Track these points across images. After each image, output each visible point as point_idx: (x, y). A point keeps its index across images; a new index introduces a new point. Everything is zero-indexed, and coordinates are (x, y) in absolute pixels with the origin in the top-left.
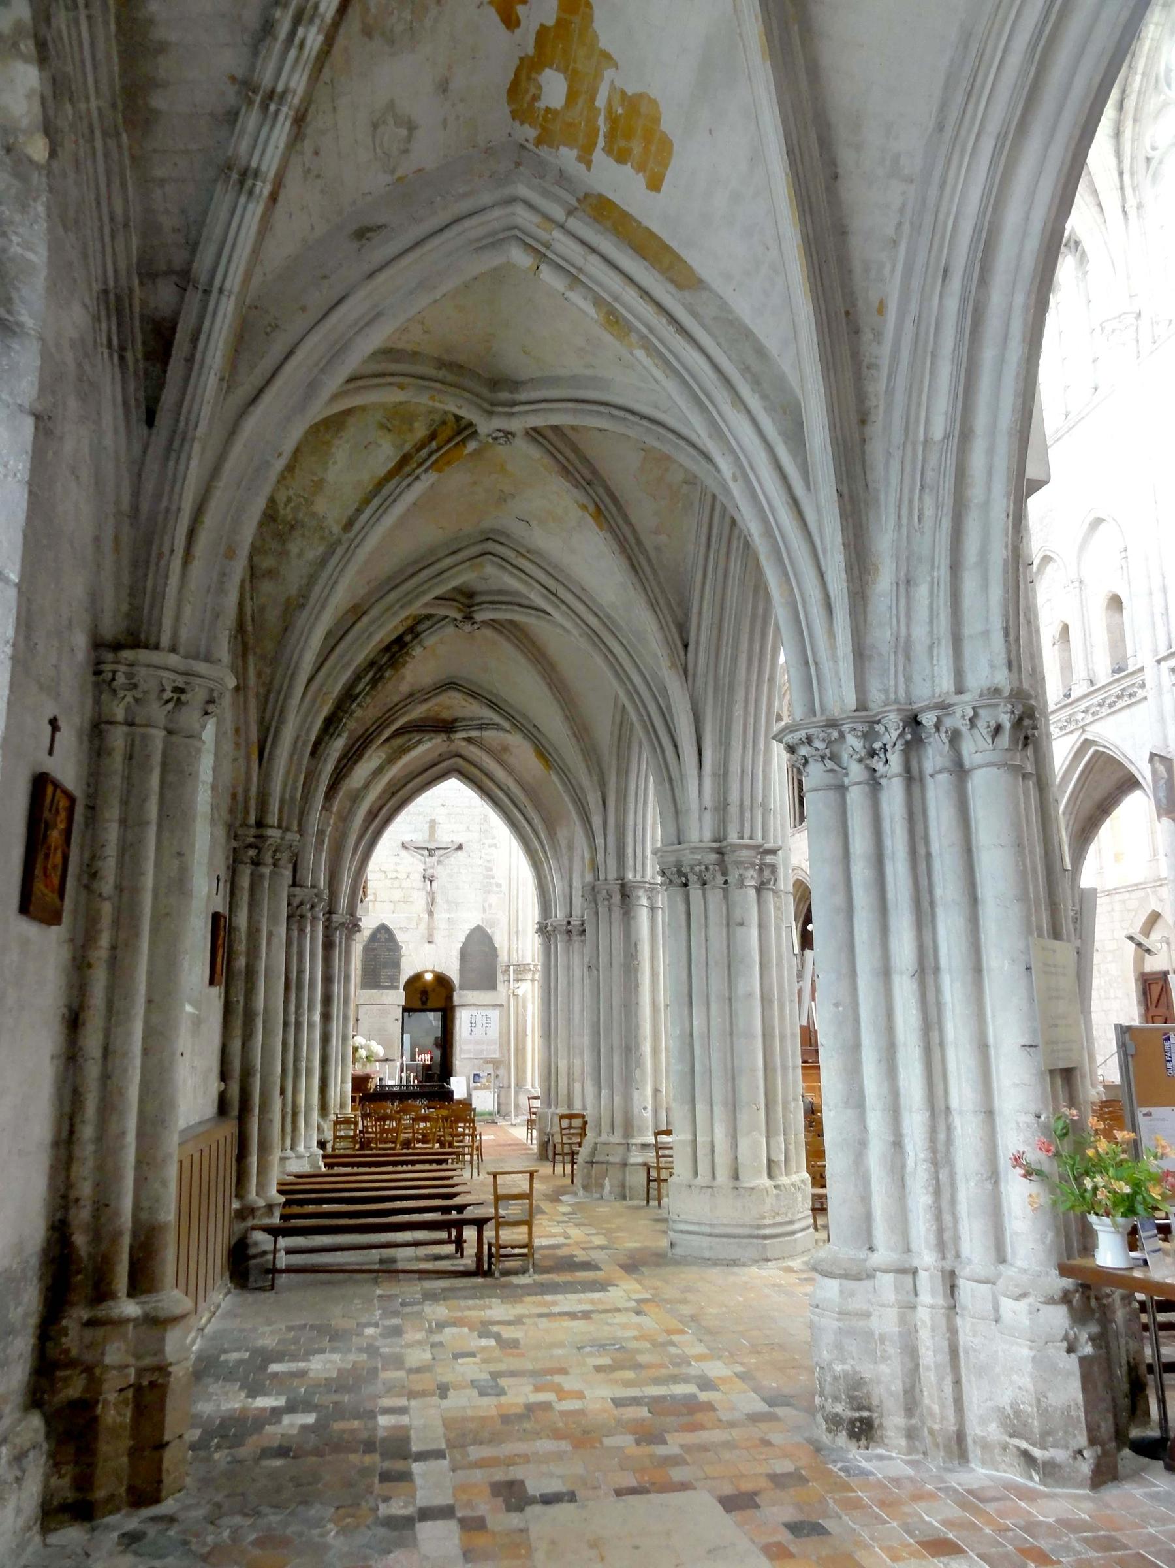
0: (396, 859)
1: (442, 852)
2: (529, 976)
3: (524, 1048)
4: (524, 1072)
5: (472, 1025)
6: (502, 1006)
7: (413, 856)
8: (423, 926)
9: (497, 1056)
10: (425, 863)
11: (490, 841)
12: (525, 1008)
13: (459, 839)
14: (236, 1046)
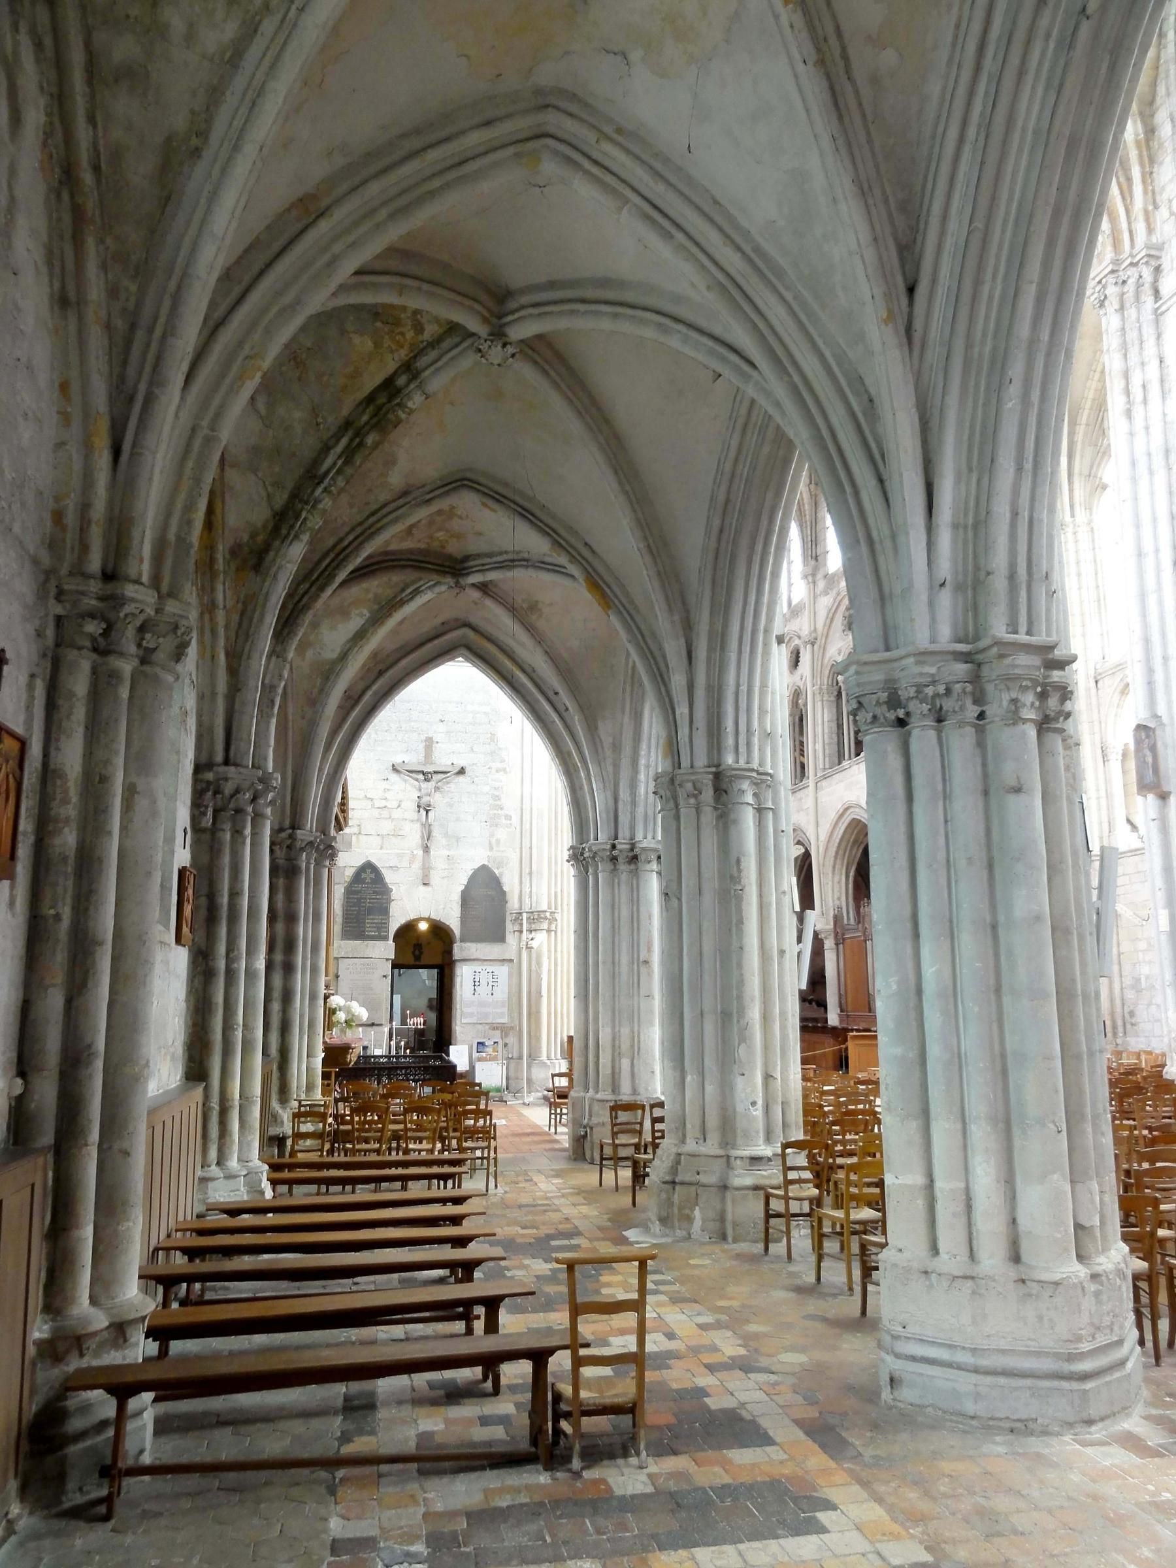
0: (385, 785)
1: (443, 776)
2: (545, 926)
3: (538, 1012)
4: (538, 1039)
5: (476, 984)
6: (511, 961)
7: (405, 781)
8: (417, 865)
9: (505, 1020)
10: (420, 790)
11: (499, 765)
12: (539, 964)
13: (460, 762)
14: (53, 1002)
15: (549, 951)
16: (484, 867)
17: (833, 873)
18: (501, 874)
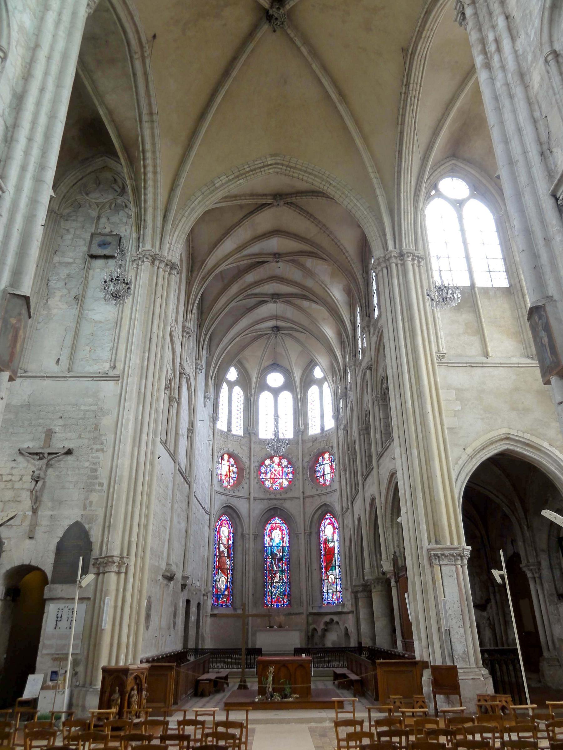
0: (13, 464)
2: (114, 568)
5: (58, 619)
6: (89, 599)
7: (28, 461)
8: (27, 523)
11: (98, 446)
13: (69, 445)
15: (117, 590)
16: (77, 524)
17: (392, 528)
18: (90, 528)
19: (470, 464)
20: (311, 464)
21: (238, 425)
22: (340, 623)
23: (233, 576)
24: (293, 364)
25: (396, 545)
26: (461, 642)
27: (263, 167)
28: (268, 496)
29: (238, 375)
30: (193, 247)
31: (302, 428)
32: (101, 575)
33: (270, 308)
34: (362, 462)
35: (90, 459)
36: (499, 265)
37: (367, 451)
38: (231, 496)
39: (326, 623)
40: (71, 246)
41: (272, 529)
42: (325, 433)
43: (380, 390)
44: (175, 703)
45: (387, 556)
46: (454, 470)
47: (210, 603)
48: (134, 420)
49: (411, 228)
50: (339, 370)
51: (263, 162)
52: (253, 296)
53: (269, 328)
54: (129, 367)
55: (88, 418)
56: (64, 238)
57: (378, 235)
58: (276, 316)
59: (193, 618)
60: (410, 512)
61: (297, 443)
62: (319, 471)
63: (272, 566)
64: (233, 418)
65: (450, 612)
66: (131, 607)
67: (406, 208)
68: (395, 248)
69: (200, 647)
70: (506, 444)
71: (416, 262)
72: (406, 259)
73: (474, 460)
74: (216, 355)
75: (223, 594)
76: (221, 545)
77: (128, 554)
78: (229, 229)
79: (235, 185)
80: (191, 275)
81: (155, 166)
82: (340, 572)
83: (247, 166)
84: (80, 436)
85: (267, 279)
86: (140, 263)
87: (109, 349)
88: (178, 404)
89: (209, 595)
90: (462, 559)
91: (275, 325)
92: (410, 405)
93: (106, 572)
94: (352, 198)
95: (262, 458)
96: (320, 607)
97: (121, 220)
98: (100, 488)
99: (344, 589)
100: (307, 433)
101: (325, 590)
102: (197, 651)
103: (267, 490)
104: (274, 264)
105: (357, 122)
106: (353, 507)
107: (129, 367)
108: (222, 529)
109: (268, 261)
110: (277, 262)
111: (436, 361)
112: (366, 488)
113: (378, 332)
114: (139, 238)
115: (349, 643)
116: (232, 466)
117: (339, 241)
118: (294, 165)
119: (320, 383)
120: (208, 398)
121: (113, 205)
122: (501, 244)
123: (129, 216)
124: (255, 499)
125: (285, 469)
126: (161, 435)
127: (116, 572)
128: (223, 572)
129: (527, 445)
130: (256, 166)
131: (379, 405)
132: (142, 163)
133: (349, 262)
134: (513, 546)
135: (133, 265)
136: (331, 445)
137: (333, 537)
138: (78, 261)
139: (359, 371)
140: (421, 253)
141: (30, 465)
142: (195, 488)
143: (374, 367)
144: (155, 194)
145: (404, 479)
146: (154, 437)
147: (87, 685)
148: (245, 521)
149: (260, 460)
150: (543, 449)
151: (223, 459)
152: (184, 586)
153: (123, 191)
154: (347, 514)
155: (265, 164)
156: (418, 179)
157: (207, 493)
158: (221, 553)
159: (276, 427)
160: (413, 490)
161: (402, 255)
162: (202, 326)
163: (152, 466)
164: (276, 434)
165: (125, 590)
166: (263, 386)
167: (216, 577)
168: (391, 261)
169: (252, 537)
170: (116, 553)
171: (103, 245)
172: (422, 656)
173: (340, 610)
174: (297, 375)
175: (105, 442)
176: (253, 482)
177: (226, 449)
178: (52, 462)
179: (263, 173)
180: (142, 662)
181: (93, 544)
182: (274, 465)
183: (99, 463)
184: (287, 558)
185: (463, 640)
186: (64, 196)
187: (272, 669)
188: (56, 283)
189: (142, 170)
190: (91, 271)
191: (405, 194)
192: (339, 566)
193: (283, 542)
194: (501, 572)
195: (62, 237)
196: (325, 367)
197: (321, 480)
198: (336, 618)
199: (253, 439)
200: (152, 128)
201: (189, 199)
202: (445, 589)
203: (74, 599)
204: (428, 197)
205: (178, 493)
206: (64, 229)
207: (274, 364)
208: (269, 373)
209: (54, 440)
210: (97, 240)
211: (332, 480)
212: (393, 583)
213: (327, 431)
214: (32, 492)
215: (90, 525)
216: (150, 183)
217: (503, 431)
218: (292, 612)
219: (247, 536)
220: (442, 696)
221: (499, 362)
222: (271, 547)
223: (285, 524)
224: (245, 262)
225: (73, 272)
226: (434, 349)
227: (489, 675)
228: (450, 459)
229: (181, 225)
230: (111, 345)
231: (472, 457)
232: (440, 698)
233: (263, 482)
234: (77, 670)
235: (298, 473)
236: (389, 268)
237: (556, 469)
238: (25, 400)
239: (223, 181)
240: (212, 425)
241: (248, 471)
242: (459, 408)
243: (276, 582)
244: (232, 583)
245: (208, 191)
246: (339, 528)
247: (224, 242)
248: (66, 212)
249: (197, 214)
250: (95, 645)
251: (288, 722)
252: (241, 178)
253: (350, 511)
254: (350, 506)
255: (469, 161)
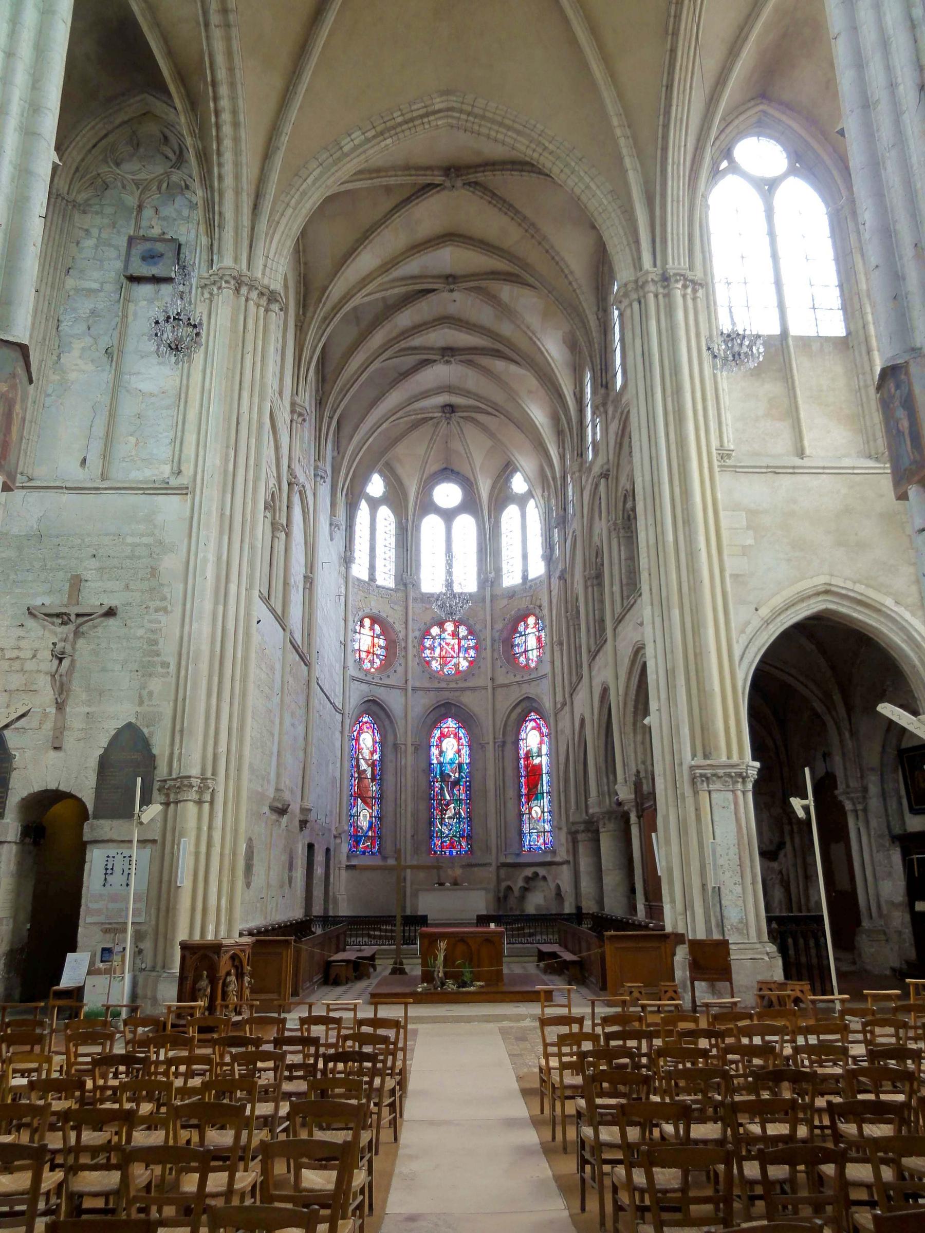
0: (20, 632)
2: (193, 795)
5: (108, 871)
6: (154, 841)
7: (44, 627)
8: (49, 725)
11: (158, 603)
15: (199, 829)
16: (129, 725)
18: (151, 733)
19: (765, 633)
20: (505, 634)
21: (386, 570)
22: (549, 878)
23: (380, 808)
24: (478, 469)
25: (640, 761)
26: (736, 905)
27: (427, 115)
28: (437, 685)
29: (385, 487)
30: (305, 264)
31: (492, 575)
32: (172, 805)
33: (438, 373)
34: (588, 630)
35: (147, 625)
36: (832, 297)
37: (596, 612)
38: (377, 685)
39: (528, 879)
40: (94, 259)
41: (443, 736)
42: (529, 584)
43: (621, 513)
44: (295, 993)
45: (625, 778)
46: (738, 642)
47: (345, 848)
48: (215, 559)
49: (684, 230)
50: (554, 478)
51: (426, 107)
52: (410, 352)
53: (436, 407)
54: (203, 471)
55: (139, 558)
56: (81, 245)
57: (625, 243)
58: (449, 387)
59: (319, 871)
60: (664, 710)
61: (484, 599)
62: (518, 645)
63: (442, 794)
64: (377, 559)
65: (721, 861)
66: (222, 855)
67: (675, 192)
68: (655, 265)
69: (331, 914)
70: (825, 601)
71: (689, 291)
72: (673, 285)
73: (771, 626)
74: (349, 452)
75: (366, 836)
76: (362, 761)
77: (214, 773)
78: (367, 231)
79: (376, 148)
80: (304, 314)
81: (234, 112)
82: (550, 802)
83: (399, 113)
84: (127, 586)
85: (434, 320)
86: (215, 291)
87: (168, 441)
88: (287, 534)
89: (343, 836)
90: (744, 782)
91: (448, 402)
92: (670, 537)
93: (180, 801)
94: (582, 173)
95: (425, 624)
96: (518, 855)
97: (179, 212)
98: (164, 670)
99: (556, 828)
100: (500, 584)
101: (526, 829)
102: (325, 920)
103: (433, 676)
104: (446, 295)
105: (594, 31)
106: (572, 703)
107: (203, 471)
108: (362, 737)
109: (434, 290)
110: (452, 291)
111: (716, 463)
112: (593, 673)
113: (622, 413)
114: (212, 245)
115: (563, 909)
116: (378, 637)
117: (558, 253)
118: (481, 112)
119: (522, 501)
120: (337, 525)
121: (165, 185)
122: (837, 259)
123: (193, 206)
124: (414, 689)
125: (463, 642)
126: (260, 585)
127: (195, 802)
128: (364, 802)
129: (860, 602)
130: (415, 114)
131: (619, 538)
132: (212, 105)
133: (574, 290)
134: (825, 761)
135: (203, 294)
136: (538, 603)
137: (540, 749)
138: (108, 287)
139: (587, 480)
140: (698, 275)
141: (47, 634)
142: (317, 671)
143: (613, 473)
144: (237, 164)
145: (656, 657)
146: (249, 589)
147: (158, 968)
148: (400, 723)
149: (423, 627)
150: (884, 609)
151: (362, 626)
152: (303, 824)
153: (180, 160)
154: (563, 713)
155: (430, 109)
156: (698, 140)
157: (337, 680)
158: (361, 773)
159: (449, 573)
160: (670, 674)
161: (665, 279)
162: (323, 402)
163: (247, 634)
164: (449, 584)
165: (210, 828)
166: (427, 506)
167: (355, 809)
168: (646, 289)
169: (410, 749)
170: (195, 771)
171: (150, 257)
172: (675, 925)
173: (548, 858)
174: (484, 487)
175: (169, 596)
176: (412, 662)
177: (367, 610)
178: (84, 628)
179: (427, 126)
180: (241, 935)
181: (157, 758)
182: (444, 635)
183: (161, 630)
184: (466, 782)
185: (740, 903)
186: (77, 169)
187: (443, 945)
188: (71, 326)
189: (213, 119)
190: (131, 307)
191: (675, 166)
192: (548, 793)
193: (460, 756)
194: (805, 802)
195: (78, 243)
196: (530, 475)
197: (522, 659)
198: (542, 871)
199: (412, 594)
200: (228, 39)
201: (297, 175)
202: (716, 827)
203: (131, 842)
204: (716, 173)
205: (291, 680)
206: (80, 228)
207: (446, 469)
208: (437, 483)
209: (84, 593)
210: (140, 249)
211: (540, 660)
212: (633, 818)
213: (532, 580)
214: (53, 676)
215: (152, 729)
216: (227, 143)
217: (821, 580)
218: (474, 861)
219: (403, 747)
220: (703, 984)
221: (821, 464)
222: (441, 764)
223: (464, 728)
224: (396, 291)
225: (100, 306)
226: (715, 443)
227: (777, 954)
228: (733, 625)
229: (284, 221)
230: (171, 434)
231: (767, 623)
232: (701, 986)
233: (428, 663)
234: (142, 946)
235: (485, 649)
236: (643, 301)
237: (904, 641)
238: (32, 527)
239: (356, 142)
240: (343, 570)
241: (403, 645)
242: (750, 541)
243: (449, 818)
244: (380, 818)
245: (330, 160)
246: (549, 735)
247: (359, 253)
248: (81, 197)
249: (311, 202)
250: (167, 911)
251: (469, 1020)
252: (387, 135)
253: (567, 708)
254: (568, 700)
255: (789, 107)
